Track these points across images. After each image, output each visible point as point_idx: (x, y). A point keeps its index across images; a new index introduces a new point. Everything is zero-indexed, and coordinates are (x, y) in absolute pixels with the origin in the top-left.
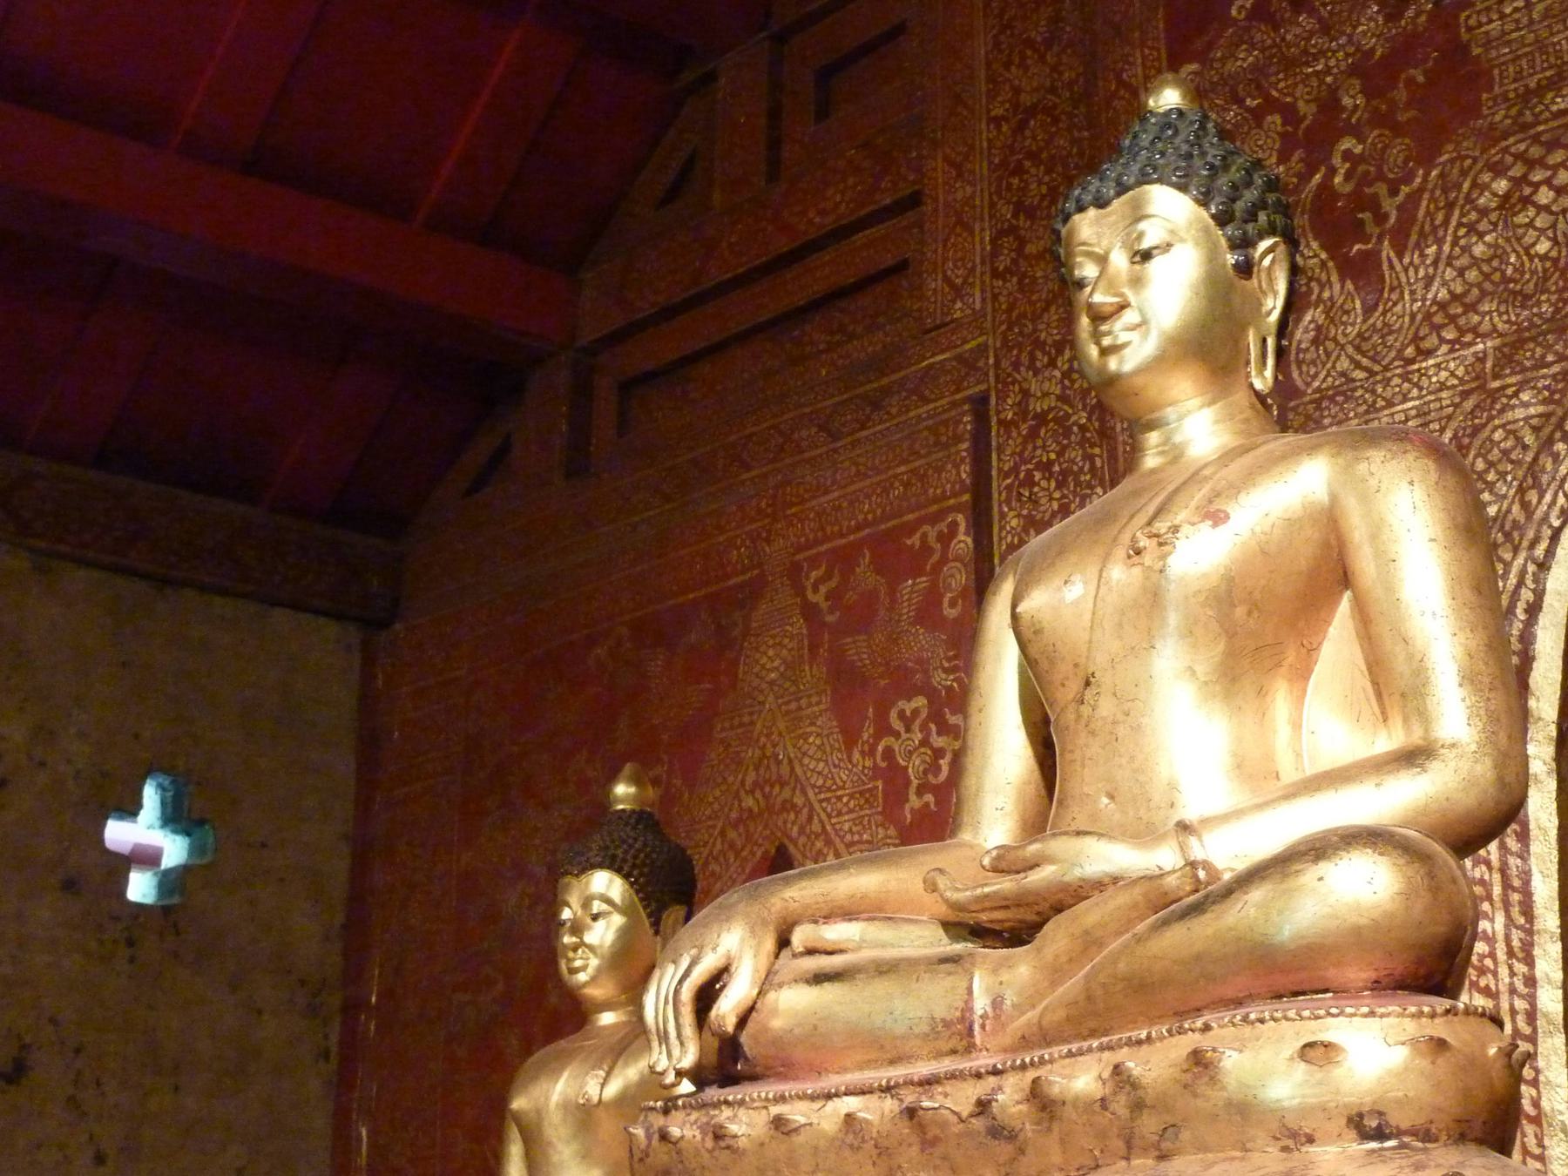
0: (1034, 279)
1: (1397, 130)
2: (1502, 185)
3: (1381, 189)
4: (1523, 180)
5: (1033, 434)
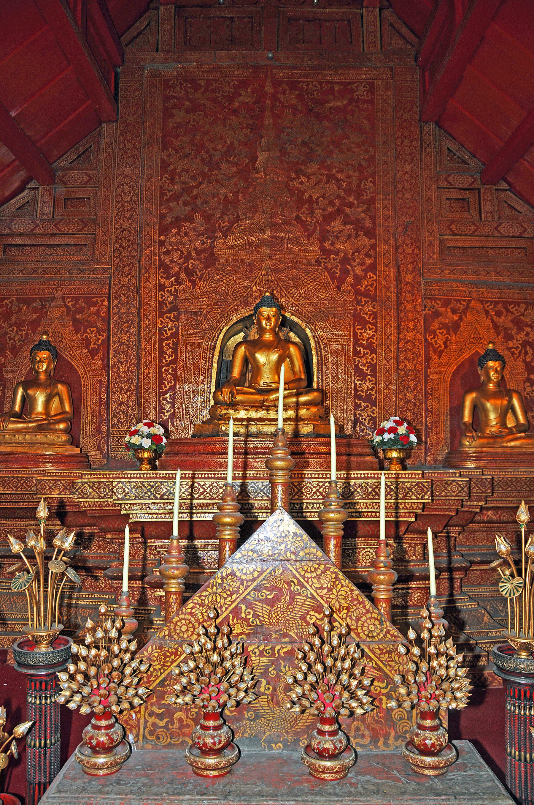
1: (201, 262)
3: (198, 271)
4: (221, 278)
5: (121, 288)
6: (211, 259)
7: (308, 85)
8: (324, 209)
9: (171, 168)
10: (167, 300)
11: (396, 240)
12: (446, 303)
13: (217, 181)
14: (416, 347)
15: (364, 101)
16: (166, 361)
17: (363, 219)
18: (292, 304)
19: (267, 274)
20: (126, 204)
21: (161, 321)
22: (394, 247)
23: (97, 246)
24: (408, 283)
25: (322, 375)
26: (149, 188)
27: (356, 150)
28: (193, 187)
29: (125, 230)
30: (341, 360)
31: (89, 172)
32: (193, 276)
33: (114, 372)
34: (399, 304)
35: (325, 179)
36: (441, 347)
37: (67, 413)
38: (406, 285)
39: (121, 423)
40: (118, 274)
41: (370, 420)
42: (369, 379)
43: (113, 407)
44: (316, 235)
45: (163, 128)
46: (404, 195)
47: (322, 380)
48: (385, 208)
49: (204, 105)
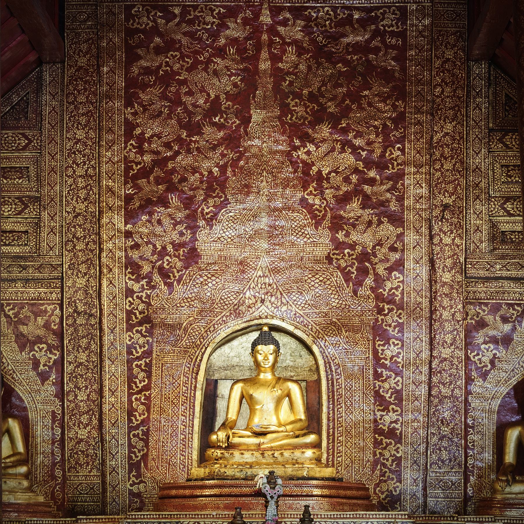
0: (78, 256)
1: (180, 260)
2: (202, 280)
4: (205, 280)
5: (76, 291)
6: (192, 256)
7: (319, 11)
8: (338, 188)
9: (138, 131)
10: (137, 309)
11: (430, 228)
12: (496, 308)
13: (198, 149)
14: (455, 367)
15: (393, 34)
16: (137, 387)
17: (388, 201)
18: (295, 314)
19: (264, 276)
20: (80, 180)
21: (130, 336)
22: (427, 237)
23: (42, 234)
24: (445, 283)
25: (333, 404)
26: (110, 159)
27: (381, 105)
28: (167, 159)
29: (79, 214)
30: (357, 385)
31: (27, 132)
32: (169, 277)
33: (70, 401)
34: (432, 312)
35: (338, 146)
36: (487, 366)
37: (20, 454)
38: (443, 286)
39: (81, 465)
40: (73, 274)
41: (393, 461)
42: (393, 409)
43: (69, 445)
44: (327, 223)
45: (126, 75)
46: (442, 165)
47: (333, 410)
48: (418, 184)
49: (180, 41)
